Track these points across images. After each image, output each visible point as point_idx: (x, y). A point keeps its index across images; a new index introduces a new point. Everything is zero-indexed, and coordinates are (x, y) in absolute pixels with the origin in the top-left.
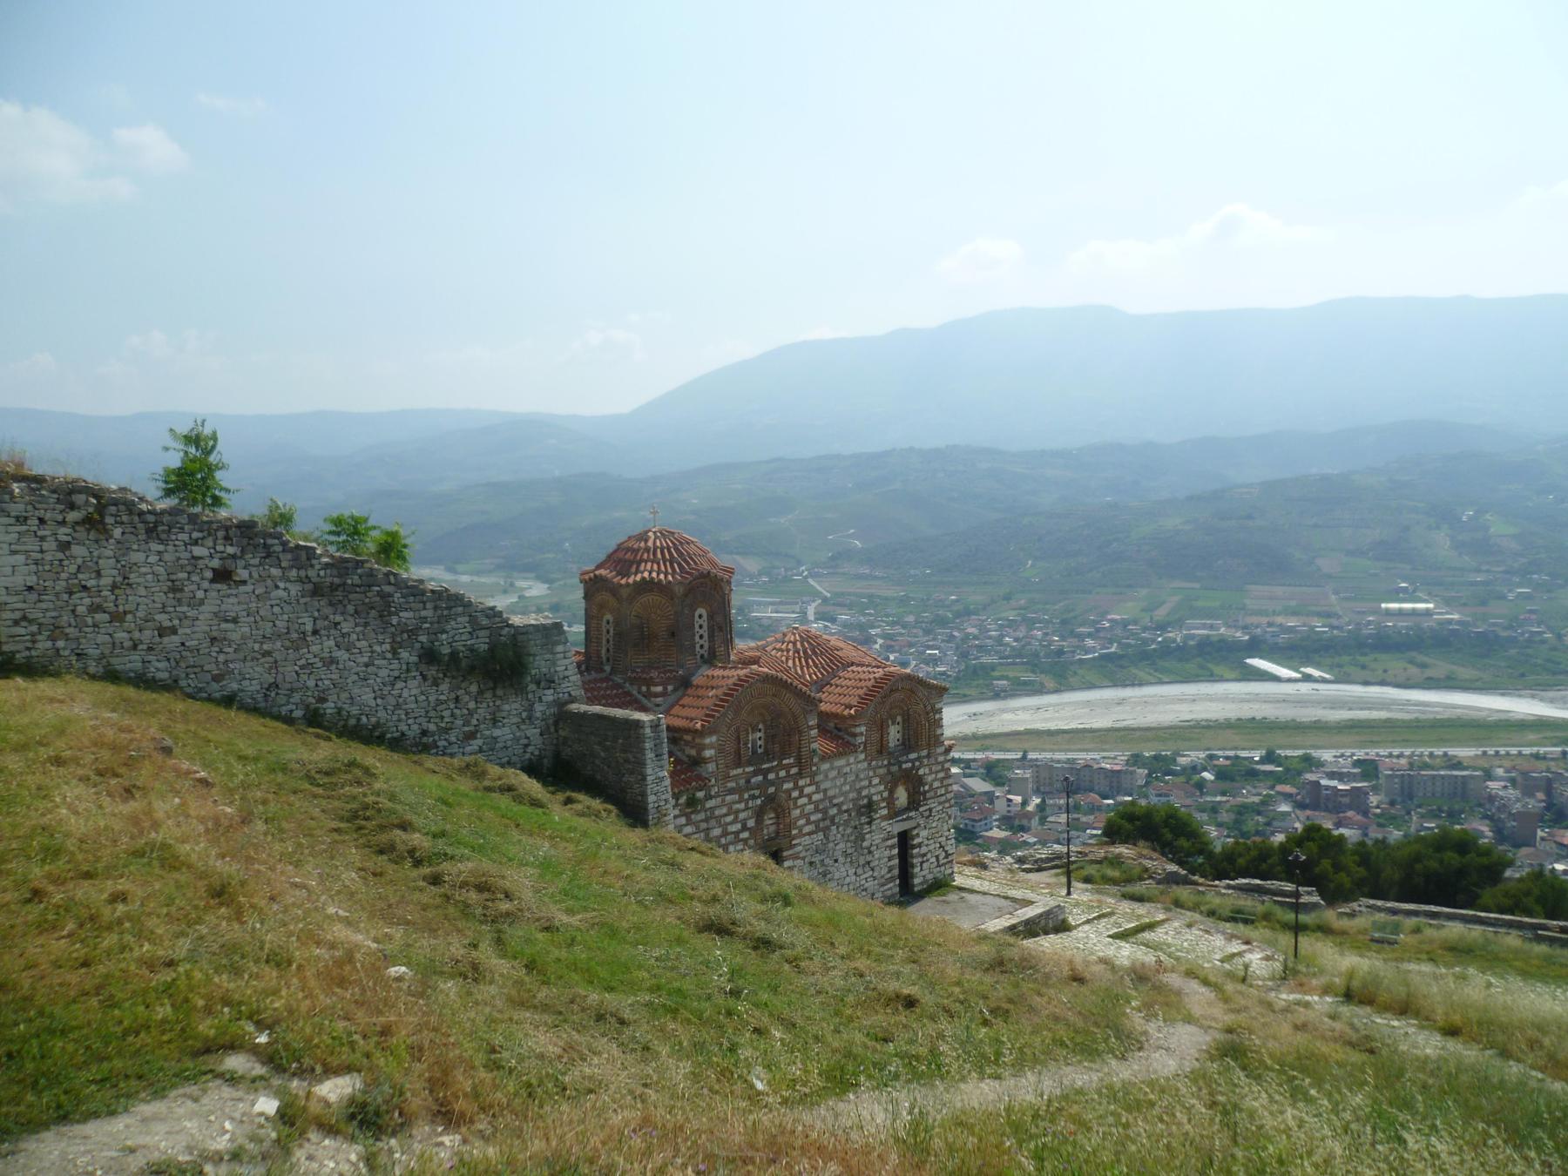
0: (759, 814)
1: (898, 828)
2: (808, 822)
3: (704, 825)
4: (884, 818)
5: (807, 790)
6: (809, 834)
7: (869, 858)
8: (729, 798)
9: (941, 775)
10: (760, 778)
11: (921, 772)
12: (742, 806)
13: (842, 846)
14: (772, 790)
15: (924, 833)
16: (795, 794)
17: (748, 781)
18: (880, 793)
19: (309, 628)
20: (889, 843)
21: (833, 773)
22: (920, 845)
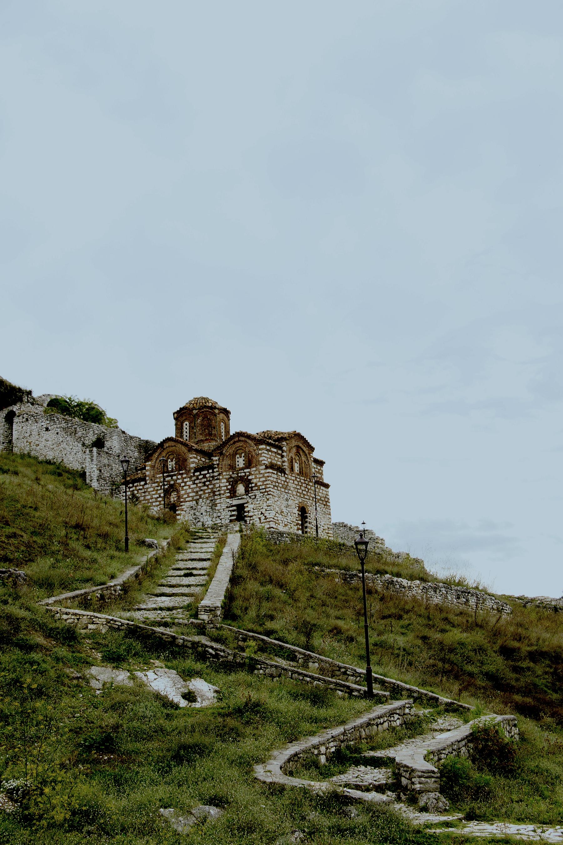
0: (167, 493)
1: (235, 502)
2: (189, 497)
3: (143, 494)
4: (228, 497)
5: (188, 483)
6: (189, 501)
7: (219, 514)
8: (154, 485)
9: (264, 479)
10: (170, 478)
11: (250, 478)
12: (159, 488)
13: (204, 508)
14: (172, 482)
15: (252, 506)
16: (183, 484)
17: (164, 479)
18: (226, 486)
19: (61, 440)
20: (231, 509)
21: (201, 477)
22: (248, 512)
